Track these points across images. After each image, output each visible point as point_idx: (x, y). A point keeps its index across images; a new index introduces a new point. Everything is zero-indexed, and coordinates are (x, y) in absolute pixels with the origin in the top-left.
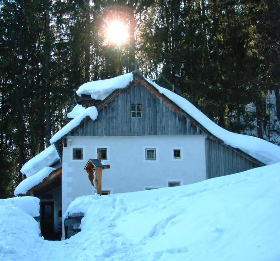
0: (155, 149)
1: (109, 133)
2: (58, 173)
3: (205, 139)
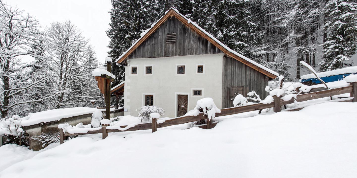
0: (178, 66)
1: (152, 56)
2: (123, 85)
3: (223, 57)
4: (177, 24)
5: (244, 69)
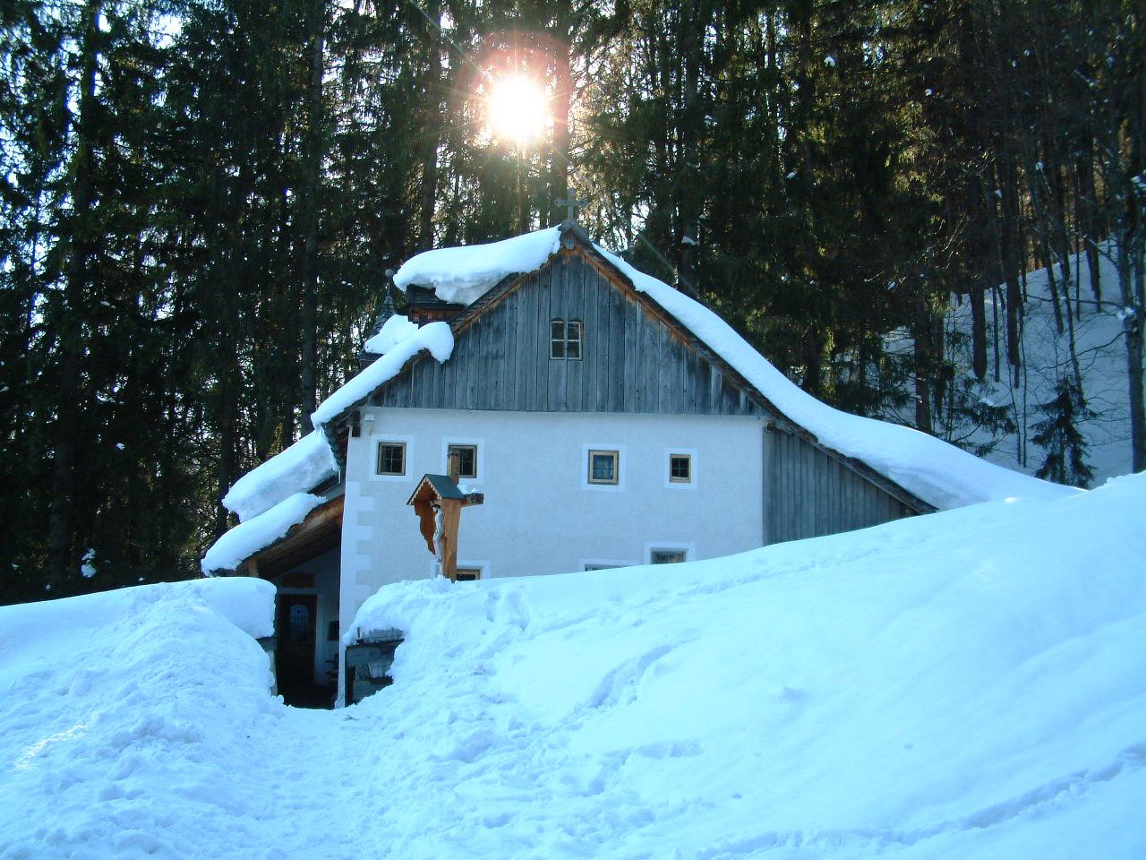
0: (617, 452)
1: (485, 402)
2: (332, 512)
3: (764, 428)
4: (590, 285)
5: (836, 476)
